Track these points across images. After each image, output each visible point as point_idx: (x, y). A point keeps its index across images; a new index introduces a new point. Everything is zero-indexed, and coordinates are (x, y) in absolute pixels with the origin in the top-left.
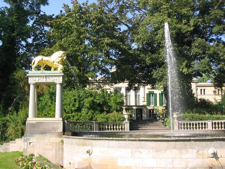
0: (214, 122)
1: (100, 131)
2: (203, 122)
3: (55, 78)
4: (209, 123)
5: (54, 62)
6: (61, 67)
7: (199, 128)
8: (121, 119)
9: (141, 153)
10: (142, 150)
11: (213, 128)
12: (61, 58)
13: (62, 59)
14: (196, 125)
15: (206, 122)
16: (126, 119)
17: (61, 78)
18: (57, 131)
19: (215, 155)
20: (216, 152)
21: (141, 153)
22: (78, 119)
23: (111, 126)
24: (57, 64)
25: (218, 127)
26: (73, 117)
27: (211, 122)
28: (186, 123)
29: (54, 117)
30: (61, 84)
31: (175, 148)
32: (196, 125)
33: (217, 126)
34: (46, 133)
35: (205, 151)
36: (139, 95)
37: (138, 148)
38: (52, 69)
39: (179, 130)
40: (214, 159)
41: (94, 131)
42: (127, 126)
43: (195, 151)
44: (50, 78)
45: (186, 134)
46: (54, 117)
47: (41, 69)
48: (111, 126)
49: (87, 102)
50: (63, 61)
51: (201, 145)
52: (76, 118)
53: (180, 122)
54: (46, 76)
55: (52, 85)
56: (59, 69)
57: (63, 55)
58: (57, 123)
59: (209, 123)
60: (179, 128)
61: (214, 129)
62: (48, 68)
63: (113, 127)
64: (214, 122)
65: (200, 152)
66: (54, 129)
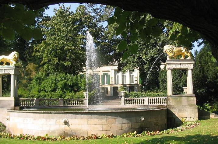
0: (149, 98)
1: (65, 105)
2: (142, 98)
3: (10, 71)
4: (146, 99)
5: (10, 59)
6: (14, 63)
7: (135, 103)
8: (83, 97)
9: (27, 120)
10: (27, 119)
11: (149, 103)
12: (14, 57)
13: (15, 57)
14: (138, 101)
15: (144, 98)
16: (123, 96)
17: (14, 70)
18: (11, 106)
19: (66, 123)
20: (67, 121)
21: (27, 120)
22: (51, 97)
23: (75, 102)
24: (12, 61)
25: (153, 103)
26: (49, 95)
27: (147, 99)
28: (130, 99)
29: (10, 97)
30: (15, 75)
31: (43, 118)
32: (138, 101)
33: (152, 101)
34: (4, 107)
35: (61, 120)
36: (133, 76)
37: (26, 117)
38: (11, 64)
39: (125, 104)
40: (66, 126)
41: (60, 106)
42: (86, 101)
43: (55, 120)
44: (7, 70)
45: (104, 108)
46: (10, 97)
47: (4, 64)
48: (75, 102)
49: (60, 85)
50: (16, 59)
51: (59, 116)
52: (50, 96)
53: (126, 99)
54: (4, 70)
55: (9, 76)
56: (13, 64)
57: (16, 55)
58: (11, 101)
59: (146, 99)
60: (125, 103)
61: (149, 104)
62: (8, 64)
63: (78, 103)
64: (149, 98)
65: (58, 121)
66: (9, 105)
